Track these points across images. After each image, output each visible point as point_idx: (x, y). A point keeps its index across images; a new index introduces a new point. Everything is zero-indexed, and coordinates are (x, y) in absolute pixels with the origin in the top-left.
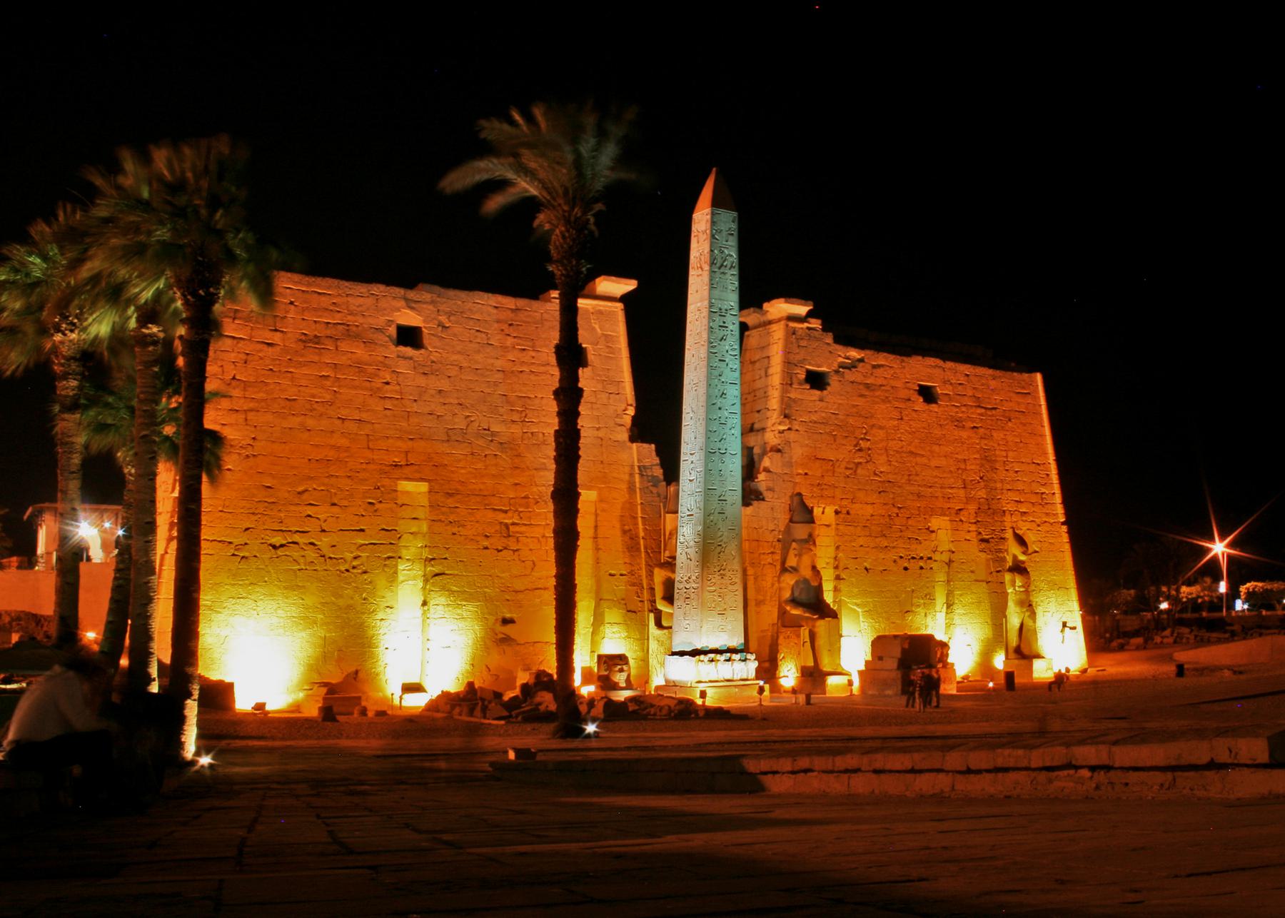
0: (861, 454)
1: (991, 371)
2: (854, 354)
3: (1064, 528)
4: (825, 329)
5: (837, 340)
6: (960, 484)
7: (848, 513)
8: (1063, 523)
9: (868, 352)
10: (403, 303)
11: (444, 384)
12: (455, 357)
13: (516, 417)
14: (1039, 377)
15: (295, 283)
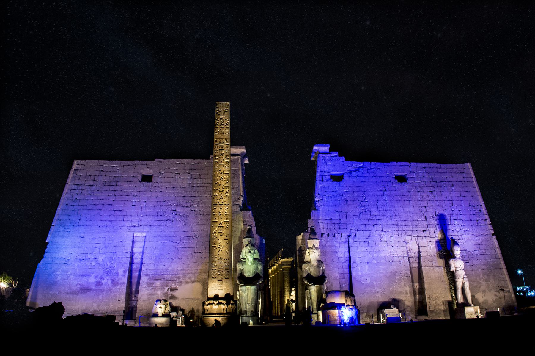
0: (362, 208)
1: (439, 165)
2: (357, 165)
3: (494, 237)
4: (340, 155)
5: (347, 160)
6: (423, 218)
7: (355, 236)
8: (493, 235)
9: (365, 163)
10: (145, 166)
11: (159, 194)
12: (165, 184)
13: (188, 204)
14: (469, 165)
15: (104, 163)
